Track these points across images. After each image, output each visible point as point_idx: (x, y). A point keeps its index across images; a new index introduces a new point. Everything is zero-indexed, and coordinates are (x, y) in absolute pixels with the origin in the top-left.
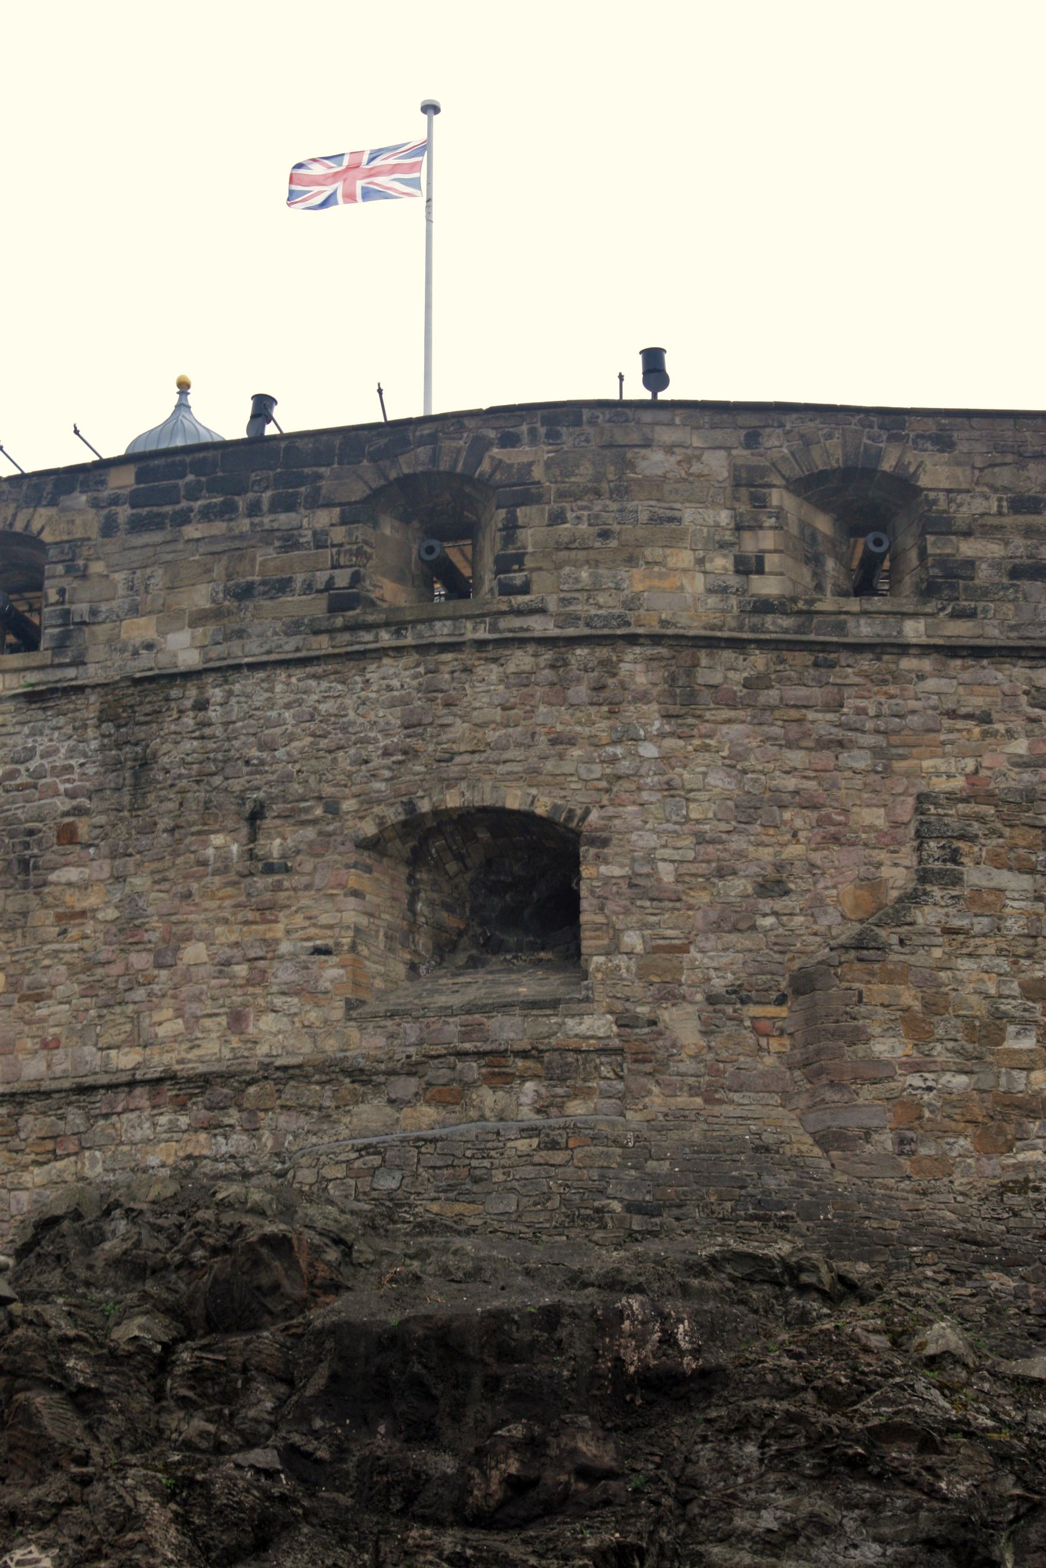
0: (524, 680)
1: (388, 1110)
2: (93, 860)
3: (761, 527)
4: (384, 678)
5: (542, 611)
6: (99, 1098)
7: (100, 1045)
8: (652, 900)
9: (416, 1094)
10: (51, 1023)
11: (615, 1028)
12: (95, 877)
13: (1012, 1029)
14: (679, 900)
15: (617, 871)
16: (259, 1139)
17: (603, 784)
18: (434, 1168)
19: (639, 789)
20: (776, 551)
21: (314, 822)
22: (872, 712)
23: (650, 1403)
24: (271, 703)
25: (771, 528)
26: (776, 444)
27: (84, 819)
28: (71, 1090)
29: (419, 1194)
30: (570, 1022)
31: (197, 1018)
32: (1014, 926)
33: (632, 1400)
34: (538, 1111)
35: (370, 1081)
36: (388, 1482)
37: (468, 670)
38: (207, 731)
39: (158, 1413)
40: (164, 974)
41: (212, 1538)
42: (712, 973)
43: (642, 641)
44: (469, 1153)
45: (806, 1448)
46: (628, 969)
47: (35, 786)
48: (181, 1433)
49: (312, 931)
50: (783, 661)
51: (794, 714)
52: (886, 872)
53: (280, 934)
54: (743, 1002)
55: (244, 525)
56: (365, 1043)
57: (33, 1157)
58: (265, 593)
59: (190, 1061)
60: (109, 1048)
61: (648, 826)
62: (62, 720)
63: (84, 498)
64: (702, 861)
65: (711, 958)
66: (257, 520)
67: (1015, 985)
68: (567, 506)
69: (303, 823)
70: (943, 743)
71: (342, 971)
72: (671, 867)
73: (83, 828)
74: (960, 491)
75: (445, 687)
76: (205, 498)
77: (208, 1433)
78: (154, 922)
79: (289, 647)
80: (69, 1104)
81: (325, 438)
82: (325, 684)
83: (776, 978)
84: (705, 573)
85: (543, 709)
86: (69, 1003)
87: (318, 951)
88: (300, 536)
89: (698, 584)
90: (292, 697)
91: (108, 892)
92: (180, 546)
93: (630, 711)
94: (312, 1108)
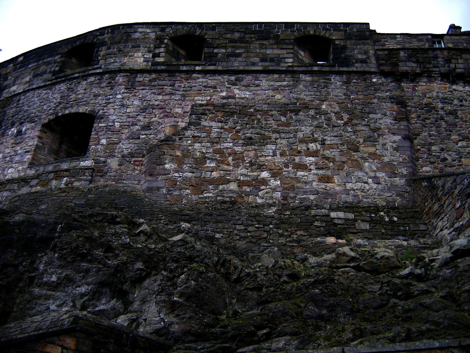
0: (92, 83)
8: (111, 132)
11: (93, 164)
13: (208, 161)
14: (119, 131)
15: (104, 125)
17: (105, 105)
20: (163, 52)
22: (183, 86)
24: (33, 97)
25: (163, 47)
26: (169, 30)
30: (82, 163)
32: (214, 135)
37: (79, 83)
42: (125, 150)
51: (161, 87)
52: (179, 124)
54: (132, 157)
67: (211, 150)
70: (202, 93)
72: (119, 124)
74: (215, 39)
93: (116, 88)
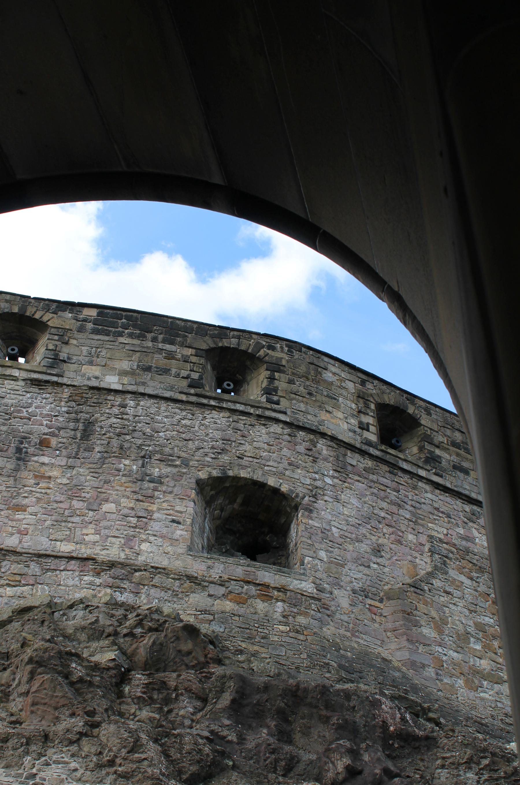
0: (277, 437)
1: (209, 599)
2: (58, 456)
3: (368, 414)
4: (213, 418)
5: (285, 413)
6: (50, 561)
7: (51, 538)
8: (330, 541)
9: (223, 595)
10: (24, 523)
11: (315, 590)
12: (57, 463)
13: (472, 639)
15: (316, 525)
16: (140, 598)
17: (310, 487)
18: (240, 627)
19: (324, 495)
21: (176, 466)
23: (402, 747)
25: (371, 416)
27: (55, 438)
28: (34, 554)
29: (234, 637)
30: (296, 582)
31: (108, 536)
33: (393, 744)
34: (284, 617)
35: (199, 584)
36: (275, 758)
38: (125, 417)
39: (120, 704)
40: (91, 513)
41: (184, 767)
43: (326, 437)
44: (256, 625)
45: (504, 778)
46: (321, 566)
47: (29, 419)
48: (135, 716)
49: (171, 512)
50: (378, 466)
53: (155, 509)
55: (150, 344)
56: (197, 567)
57: (7, 582)
58: (157, 371)
59: (102, 555)
60: (55, 540)
61: (328, 511)
62: (48, 395)
63: (70, 315)
64: (349, 532)
65: (354, 574)
66: (155, 344)
68: (295, 379)
69: (170, 465)
71: (186, 533)
73: (54, 442)
75: (242, 429)
76: (130, 329)
77: (154, 718)
78: (88, 489)
79: (168, 394)
80: (32, 561)
81: (189, 323)
82: (184, 413)
83: (378, 591)
84: (347, 423)
85: (285, 449)
86: (36, 515)
87: (173, 521)
88: (176, 355)
89: (346, 426)
90: (169, 414)
91: (63, 472)
92: (117, 344)
94: (169, 589)
